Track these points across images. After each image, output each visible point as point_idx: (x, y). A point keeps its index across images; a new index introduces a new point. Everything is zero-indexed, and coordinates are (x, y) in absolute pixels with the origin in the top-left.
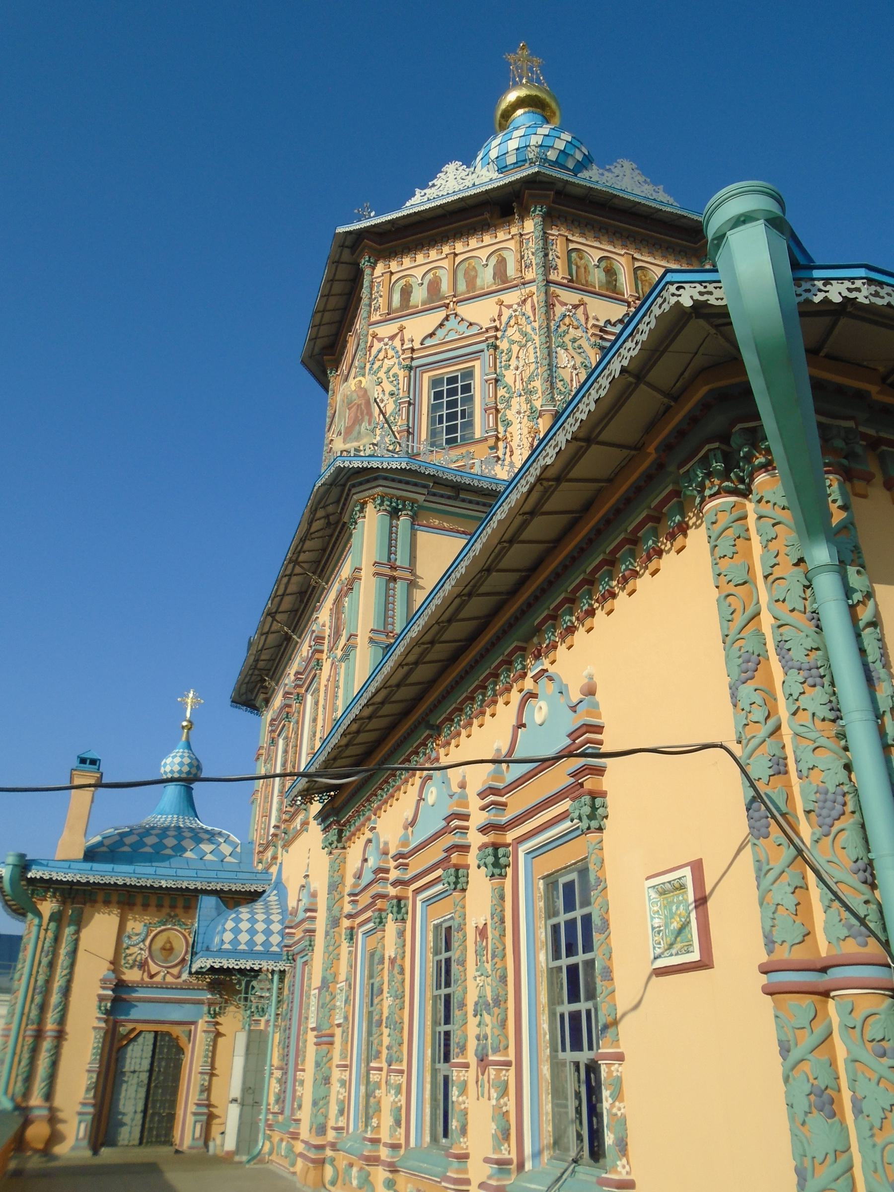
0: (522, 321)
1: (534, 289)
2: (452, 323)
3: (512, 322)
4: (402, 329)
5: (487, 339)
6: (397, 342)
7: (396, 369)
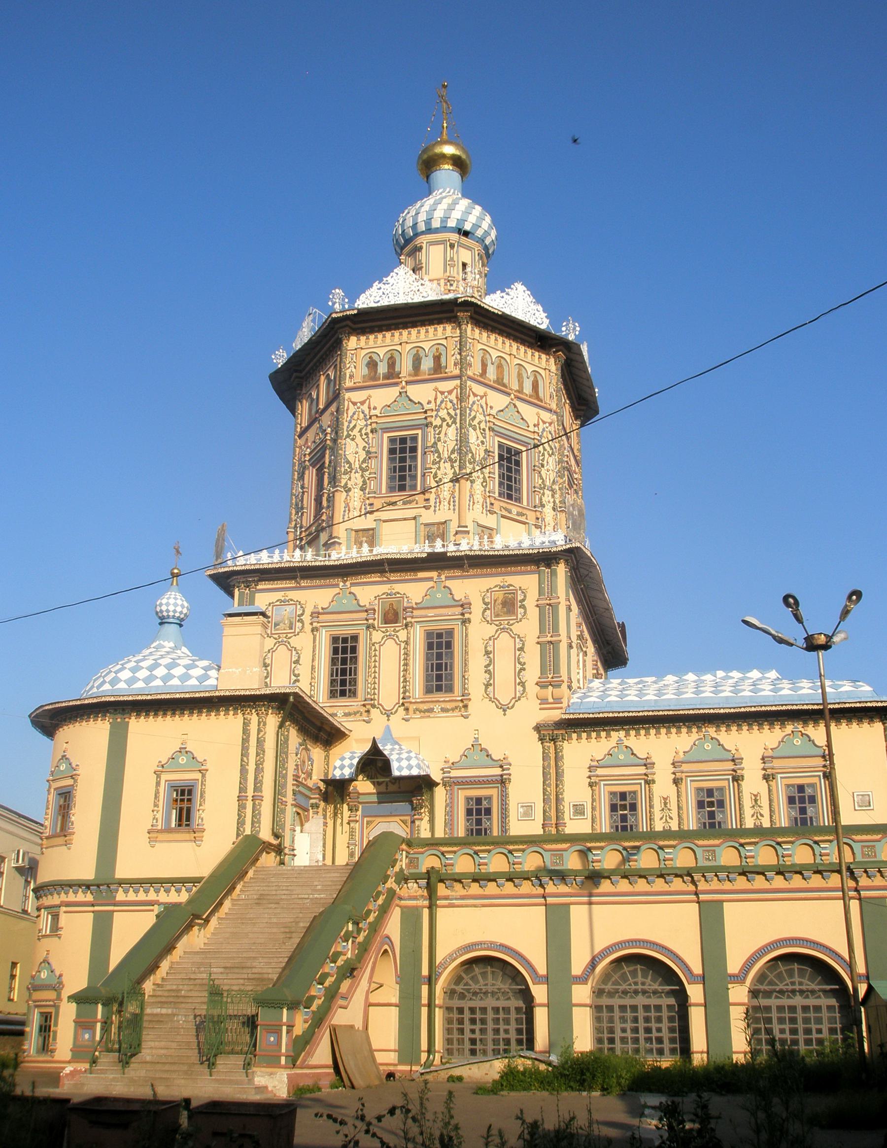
0: (449, 405)
1: (458, 382)
3: (443, 405)
4: (369, 397)
5: (426, 418)
6: (365, 408)
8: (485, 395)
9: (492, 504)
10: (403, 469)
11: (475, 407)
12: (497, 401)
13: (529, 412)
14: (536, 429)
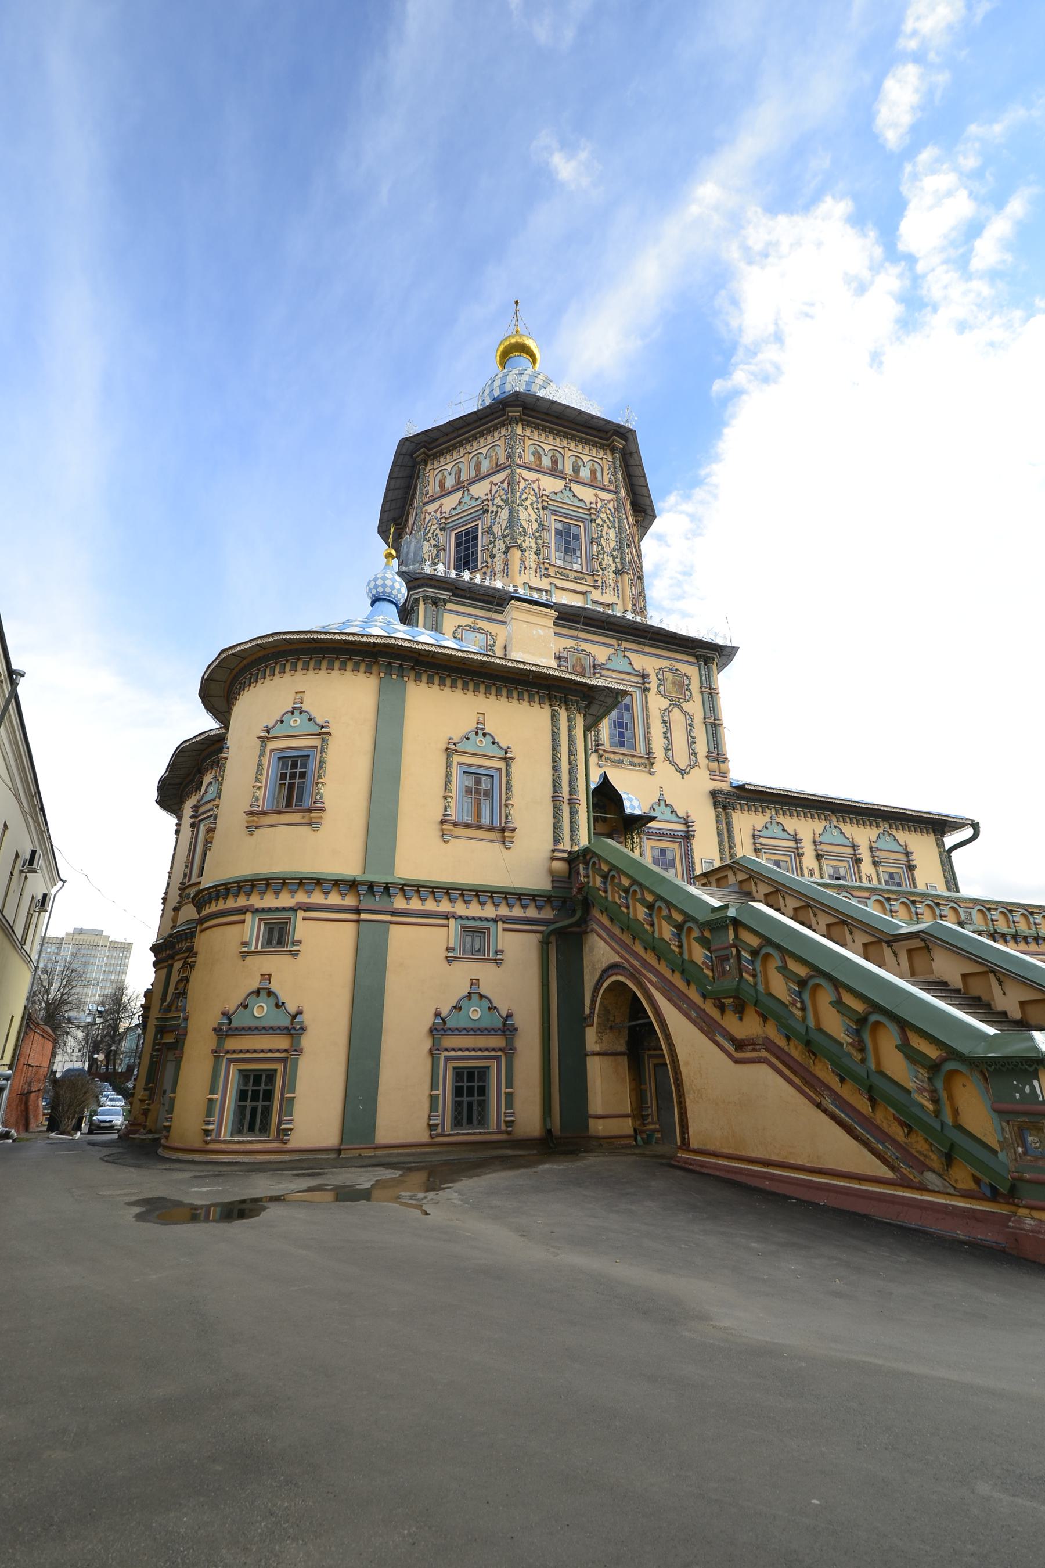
0: (502, 492)
2: (467, 499)
6: (438, 515)
7: (438, 531)
8: (538, 480)
9: (547, 569)
10: (467, 556)
11: (527, 491)
12: (551, 485)
13: (587, 494)
14: (593, 506)
